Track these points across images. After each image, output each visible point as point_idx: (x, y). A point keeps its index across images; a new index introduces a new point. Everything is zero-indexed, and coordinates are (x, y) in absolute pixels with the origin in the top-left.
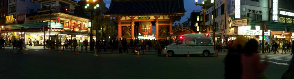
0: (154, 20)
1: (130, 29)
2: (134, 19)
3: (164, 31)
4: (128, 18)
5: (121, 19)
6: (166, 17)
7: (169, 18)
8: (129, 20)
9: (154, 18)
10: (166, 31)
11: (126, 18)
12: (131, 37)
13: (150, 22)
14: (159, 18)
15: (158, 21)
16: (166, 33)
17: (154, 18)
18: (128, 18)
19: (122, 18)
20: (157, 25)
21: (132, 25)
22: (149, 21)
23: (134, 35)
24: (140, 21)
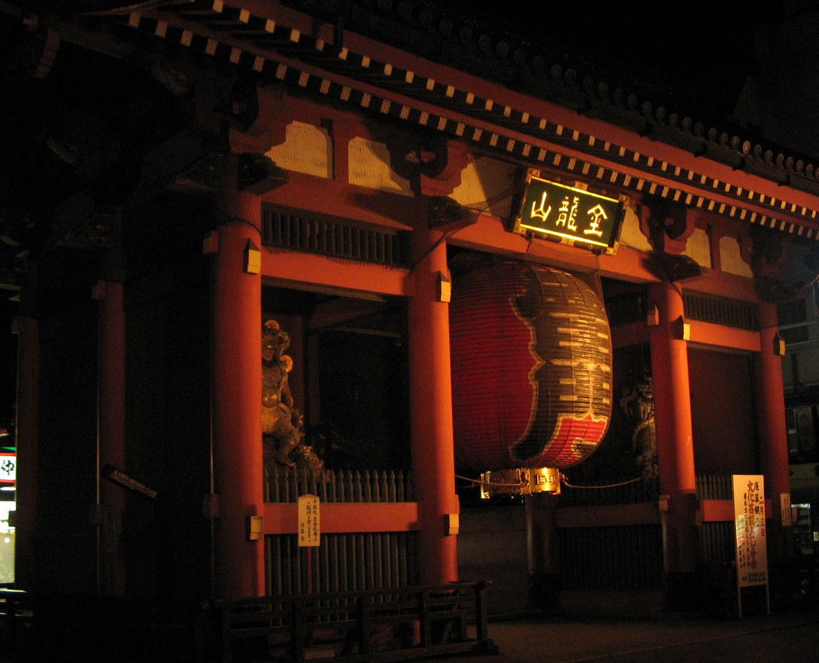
18: (369, 169)
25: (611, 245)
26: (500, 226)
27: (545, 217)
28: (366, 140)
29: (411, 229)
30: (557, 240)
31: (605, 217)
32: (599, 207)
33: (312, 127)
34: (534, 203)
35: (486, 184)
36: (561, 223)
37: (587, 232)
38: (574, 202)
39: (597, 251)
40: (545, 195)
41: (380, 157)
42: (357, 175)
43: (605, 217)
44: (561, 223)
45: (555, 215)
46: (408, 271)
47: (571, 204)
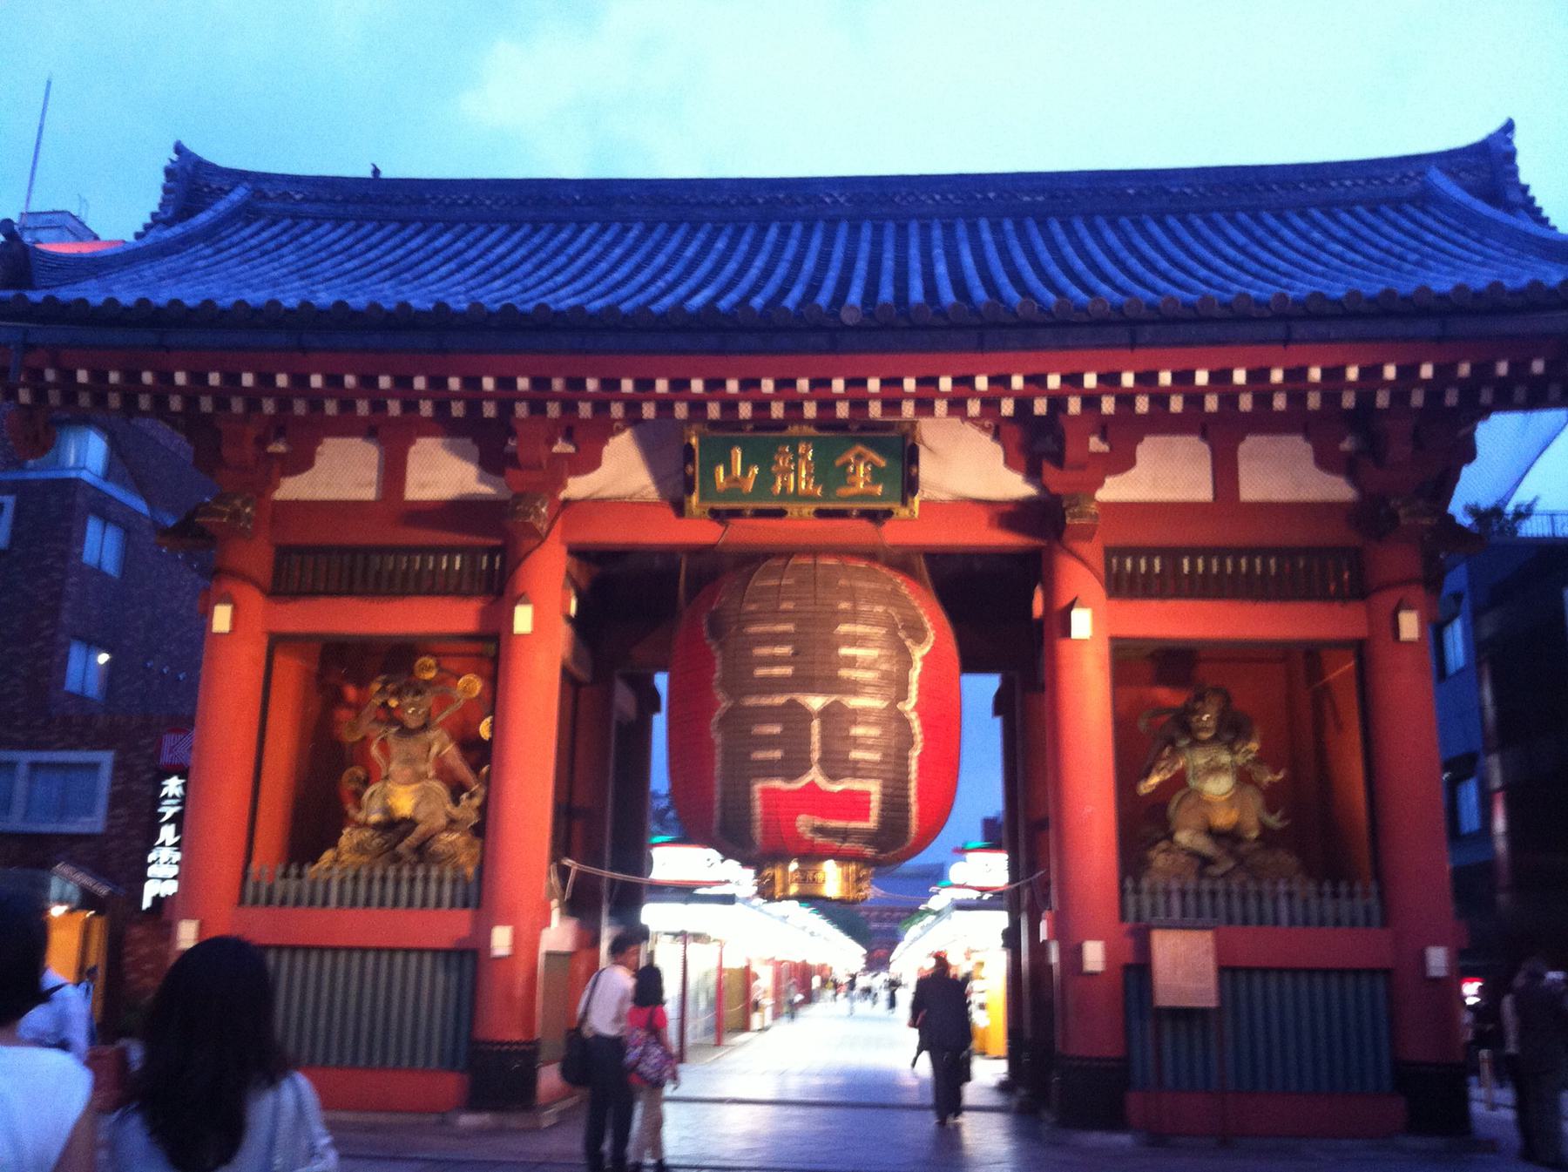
0: (1010, 514)
1: (484, 730)
2: (577, 487)
3: (1218, 787)
4: (442, 473)
5: (292, 488)
6: (1279, 474)
7: (1338, 489)
8: (458, 512)
9: (1016, 487)
10: (1244, 777)
11: (393, 472)
12: (479, 896)
13: (901, 561)
14: (1114, 490)
15: (1092, 550)
16: (1249, 816)
17: (1016, 487)
18: (442, 473)
19: (302, 462)
20: (1082, 623)
21: (523, 620)
22: (889, 535)
23: (562, 845)
24: (697, 530)
25: (904, 503)
26: (670, 513)
27: (750, 485)
28: (440, 440)
29: (499, 542)
30: (780, 513)
31: (883, 464)
32: (860, 448)
33: (358, 441)
34: (721, 470)
35: (652, 452)
36: (784, 488)
37: (844, 491)
38: (801, 450)
39: (877, 517)
40: (737, 455)
41: (463, 455)
42: (423, 486)
43: (883, 464)
44: (784, 488)
45: (765, 480)
46: (492, 598)
47: (797, 457)
